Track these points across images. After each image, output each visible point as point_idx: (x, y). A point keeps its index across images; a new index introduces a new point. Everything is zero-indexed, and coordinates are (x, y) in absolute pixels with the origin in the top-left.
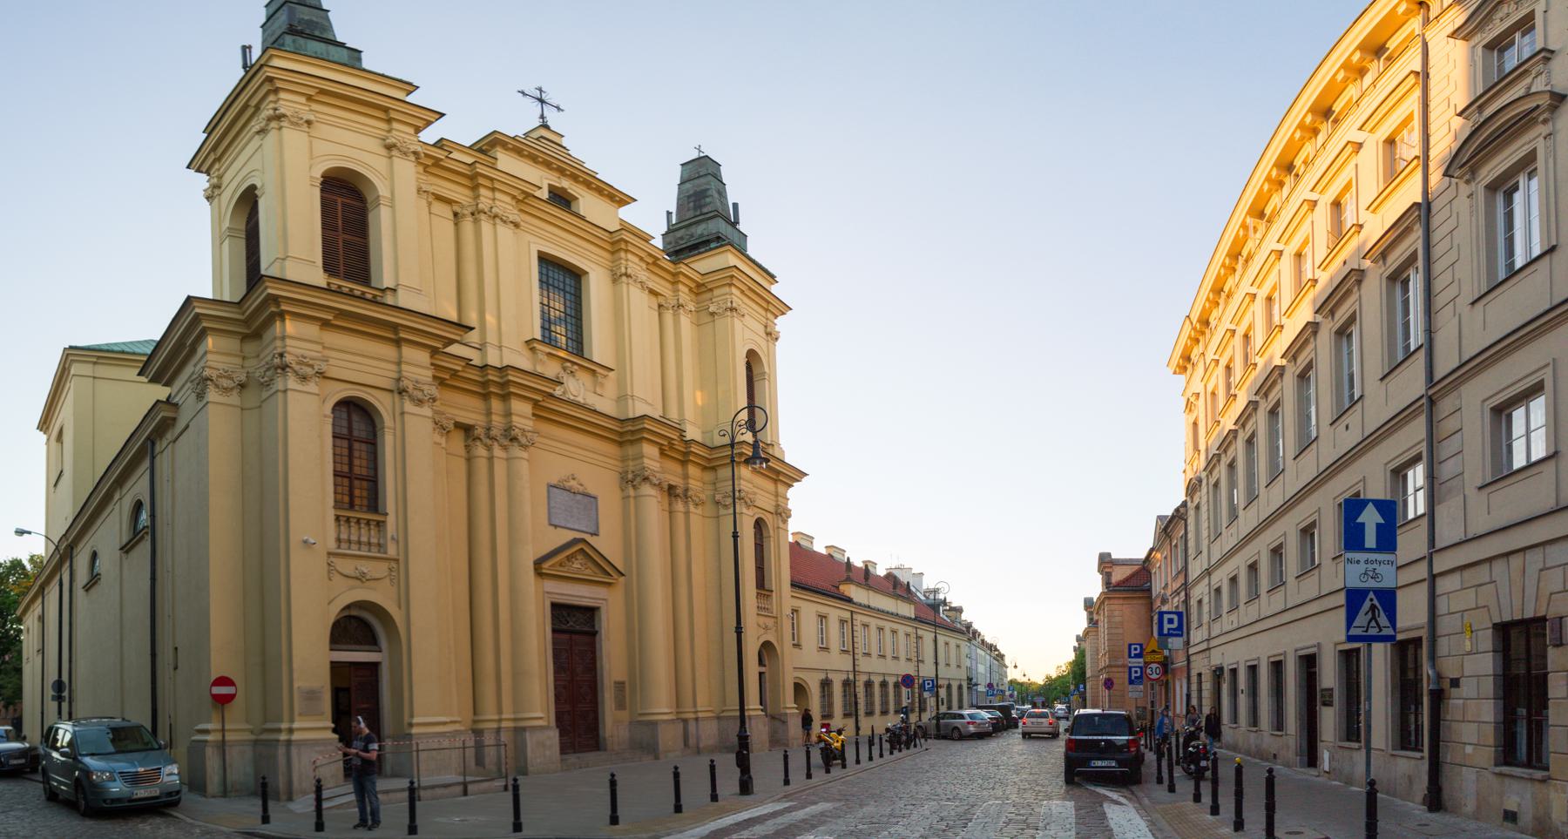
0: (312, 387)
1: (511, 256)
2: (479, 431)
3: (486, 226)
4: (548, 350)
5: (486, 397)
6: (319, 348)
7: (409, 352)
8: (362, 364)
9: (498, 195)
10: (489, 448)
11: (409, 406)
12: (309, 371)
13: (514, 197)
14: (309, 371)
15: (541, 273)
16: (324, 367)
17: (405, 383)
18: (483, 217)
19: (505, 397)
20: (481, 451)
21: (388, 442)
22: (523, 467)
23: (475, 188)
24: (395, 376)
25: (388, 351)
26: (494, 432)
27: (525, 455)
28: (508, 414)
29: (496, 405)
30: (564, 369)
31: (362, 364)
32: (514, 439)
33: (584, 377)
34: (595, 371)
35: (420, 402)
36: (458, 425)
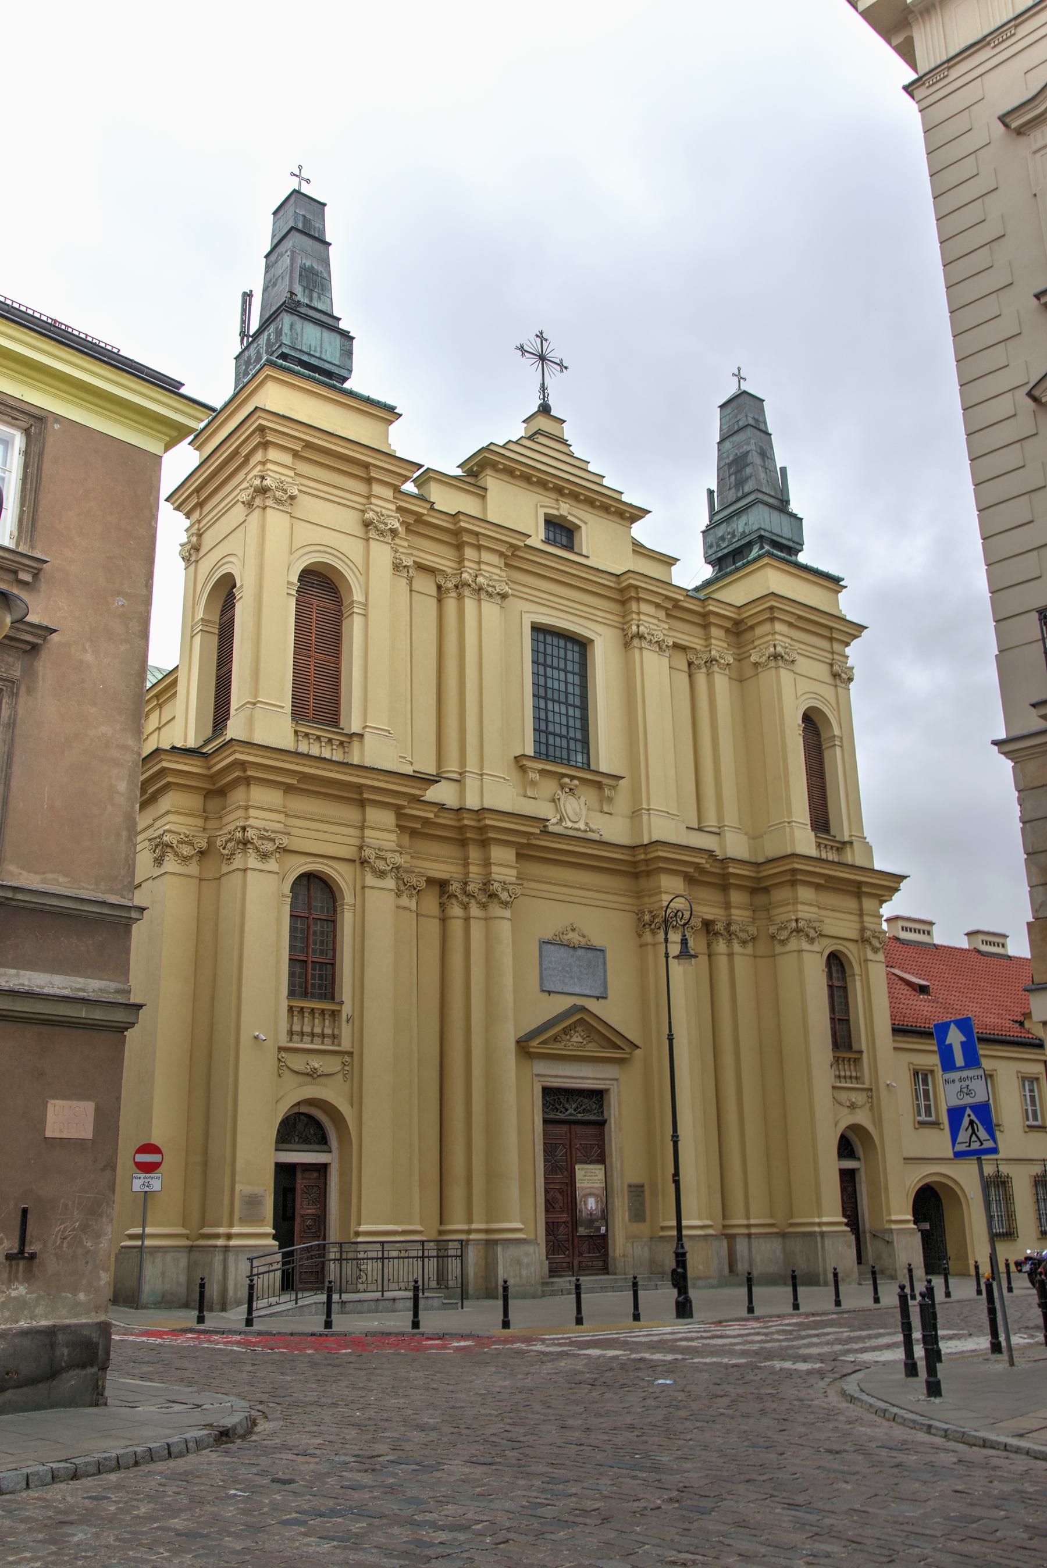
0: (272, 865)
1: (497, 640)
2: (455, 887)
3: (470, 604)
4: (540, 766)
5: (463, 843)
7: (374, 815)
8: (323, 836)
9: (486, 556)
10: (465, 907)
11: (370, 880)
12: (269, 846)
13: (501, 554)
14: (269, 846)
15: (535, 651)
16: (285, 841)
17: (367, 853)
18: (466, 592)
19: (484, 844)
20: (456, 911)
21: (347, 920)
22: (504, 929)
23: (459, 547)
24: (356, 842)
25: (351, 814)
26: (471, 888)
27: (507, 913)
28: (487, 863)
29: (474, 854)
30: (562, 787)
31: (323, 836)
32: (493, 896)
33: (588, 795)
34: (602, 784)
35: (381, 874)
36: (430, 881)
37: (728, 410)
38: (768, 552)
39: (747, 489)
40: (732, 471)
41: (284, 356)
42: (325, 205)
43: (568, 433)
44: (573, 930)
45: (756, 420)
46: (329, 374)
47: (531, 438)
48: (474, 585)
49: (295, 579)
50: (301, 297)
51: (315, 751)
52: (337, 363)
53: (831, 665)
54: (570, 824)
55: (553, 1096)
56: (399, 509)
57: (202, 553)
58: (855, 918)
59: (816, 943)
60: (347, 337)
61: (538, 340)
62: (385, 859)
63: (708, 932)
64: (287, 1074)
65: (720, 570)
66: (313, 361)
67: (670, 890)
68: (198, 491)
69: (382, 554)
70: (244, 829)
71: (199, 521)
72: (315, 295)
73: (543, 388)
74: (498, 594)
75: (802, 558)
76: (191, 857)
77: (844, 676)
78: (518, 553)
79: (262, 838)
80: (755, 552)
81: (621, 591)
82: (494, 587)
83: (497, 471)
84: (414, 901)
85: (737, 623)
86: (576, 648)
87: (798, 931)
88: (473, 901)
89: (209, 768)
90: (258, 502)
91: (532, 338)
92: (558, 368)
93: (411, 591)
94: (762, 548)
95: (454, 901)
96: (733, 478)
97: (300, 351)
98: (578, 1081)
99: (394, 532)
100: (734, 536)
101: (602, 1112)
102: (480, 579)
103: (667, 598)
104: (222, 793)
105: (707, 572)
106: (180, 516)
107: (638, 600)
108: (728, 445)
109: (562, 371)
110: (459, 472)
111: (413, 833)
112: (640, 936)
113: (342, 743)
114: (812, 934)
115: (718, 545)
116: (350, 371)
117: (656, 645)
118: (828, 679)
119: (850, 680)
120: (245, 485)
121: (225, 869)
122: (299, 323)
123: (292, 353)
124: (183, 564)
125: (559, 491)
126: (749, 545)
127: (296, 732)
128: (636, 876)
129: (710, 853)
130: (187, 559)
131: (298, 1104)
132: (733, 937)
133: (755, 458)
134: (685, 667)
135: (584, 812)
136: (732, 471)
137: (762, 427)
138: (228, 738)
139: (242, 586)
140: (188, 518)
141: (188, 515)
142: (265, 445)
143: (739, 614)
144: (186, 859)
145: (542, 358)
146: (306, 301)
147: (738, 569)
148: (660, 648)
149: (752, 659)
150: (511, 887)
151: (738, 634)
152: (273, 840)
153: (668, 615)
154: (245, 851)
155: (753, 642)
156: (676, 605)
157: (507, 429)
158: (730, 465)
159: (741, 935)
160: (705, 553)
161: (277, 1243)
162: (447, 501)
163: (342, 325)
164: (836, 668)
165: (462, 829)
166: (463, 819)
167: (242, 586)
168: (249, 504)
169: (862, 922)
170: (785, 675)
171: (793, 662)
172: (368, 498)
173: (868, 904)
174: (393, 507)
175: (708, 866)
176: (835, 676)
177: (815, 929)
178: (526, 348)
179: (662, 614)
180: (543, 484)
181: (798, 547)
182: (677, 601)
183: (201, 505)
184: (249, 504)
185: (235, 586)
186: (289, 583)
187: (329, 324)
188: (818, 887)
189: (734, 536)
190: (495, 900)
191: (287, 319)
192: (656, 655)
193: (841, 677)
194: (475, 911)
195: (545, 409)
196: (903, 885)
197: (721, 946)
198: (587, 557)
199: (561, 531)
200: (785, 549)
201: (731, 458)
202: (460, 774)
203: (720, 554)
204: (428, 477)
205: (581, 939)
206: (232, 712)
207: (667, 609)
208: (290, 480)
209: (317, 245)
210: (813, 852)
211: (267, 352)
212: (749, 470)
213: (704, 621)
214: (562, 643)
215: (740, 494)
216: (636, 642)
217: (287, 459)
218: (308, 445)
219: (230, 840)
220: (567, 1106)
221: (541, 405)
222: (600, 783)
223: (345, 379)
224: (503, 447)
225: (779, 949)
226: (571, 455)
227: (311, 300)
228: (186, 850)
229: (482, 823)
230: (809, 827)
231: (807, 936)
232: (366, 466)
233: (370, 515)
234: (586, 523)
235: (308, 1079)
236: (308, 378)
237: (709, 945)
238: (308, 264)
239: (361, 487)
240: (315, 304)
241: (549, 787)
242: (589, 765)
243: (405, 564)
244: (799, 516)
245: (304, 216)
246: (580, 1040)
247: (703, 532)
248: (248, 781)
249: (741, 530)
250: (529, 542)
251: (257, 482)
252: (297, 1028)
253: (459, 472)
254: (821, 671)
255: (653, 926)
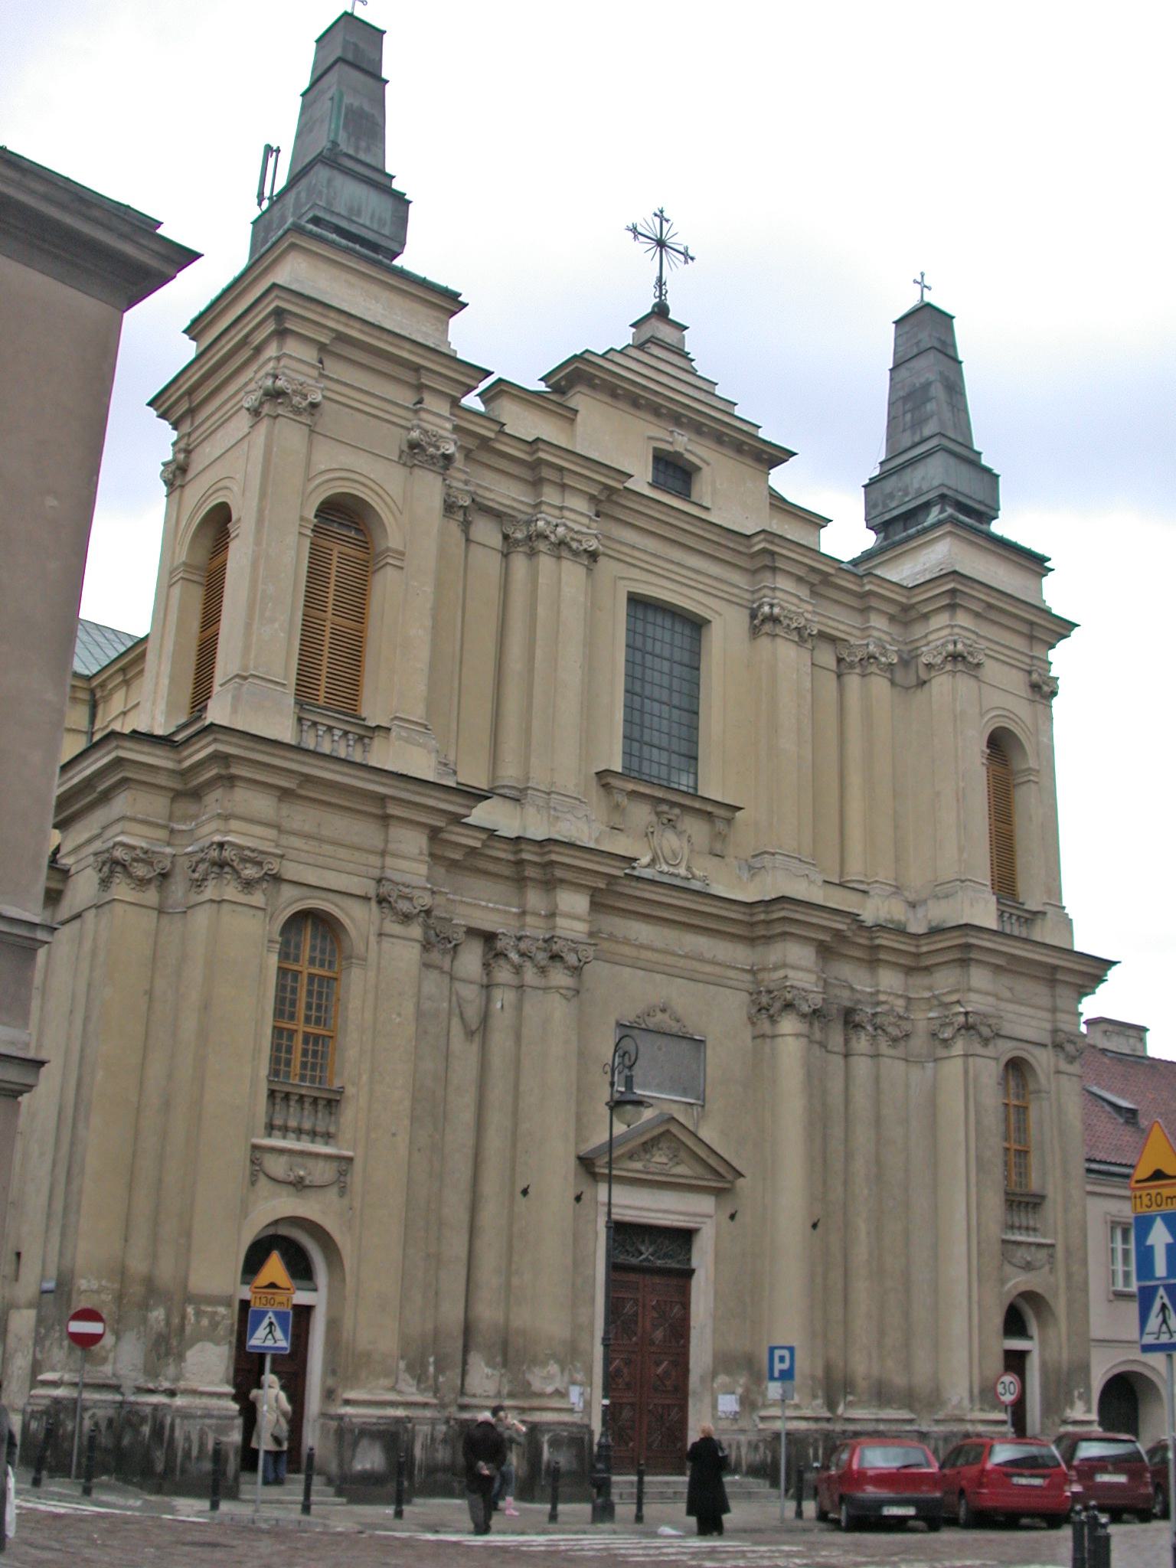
0: (258, 898)
3: (545, 562)
5: (520, 882)
6: (272, 833)
10: (518, 970)
13: (592, 498)
16: (275, 866)
18: (542, 546)
19: (550, 885)
29: (534, 899)
30: (658, 814)
31: (330, 860)
32: (555, 957)
35: (406, 918)
36: (472, 932)
37: (906, 328)
38: (951, 516)
39: (927, 432)
40: (908, 406)
41: (316, 221)
42: (384, 32)
43: (691, 343)
44: (663, 1010)
45: (943, 343)
46: (374, 247)
47: (640, 347)
48: (553, 538)
49: (310, 514)
50: (344, 147)
51: (326, 748)
52: (386, 231)
53: (1030, 673)
54: (665, 868)
55: (623, 1233)
56: (457, 429)
57: (191, 474)
58: (1047, 1015)
59: (991, 1047)
60: (401, 202)
61: (657, 220)
62: (411, 899)
63: (846, 1023)
64: (263, 1180)
65: (885, 538)
66: (353, 229)
67: (796, 964)
68: (190, 392)
69: (429, 489)
70: (221, 845)
71: (189, 434)
72: (363, 144)
73: (660, 283)
74: (585, 551)
75: (996, 528)
76: (150, 881)
77: (1046, 688)
78: (614, 498)
79: (244, 860)
80: (934, 515)
81: (753, 556)
82: (580, 542)
83: (594, 387)
84: (448, 959)
85: (906, 609)
86: (687, 632)
87: (968, 1027)
88: (528, 964)
89: (180, 762)
90: (266, 409)
91: (650, 217)
92: (682, 258)
93: (468, 540)
94: (942, 511)
95: (502, 962)
96: (908, 416)
97: (338, 214)
98: (660, 1215)
99: (448, 458)
100: (906, 494)
101: (689, 1260)
102: (561, 530)
103: (813, 569)
104: (196, 794)
105: (868, 540)
106: (165, 425)
107: (774, 569)
108: (903, 373)
109: (686, 262)
110: (542, 387)
111: (453, 865)
112: (753, 1024)
113: (361, 738)
114: (986, 1031)
115: (885, 505)
116: (403, 244)
117: (795, 633)
118: (1024, 691)
119: (1054, 693)
120: (253, 386)
121: (196, 898)
122: (340, 180)
123: (328, 217)
124: (164, 489)
125: (677, 419)
126: (926, 506)
127: (300, 720)
128: (752, 941)
129: (854, 917)
130: (170, 484)
131: (276, 1222)
132: (880, 1032)
133: (938, 391)
134: (833, 665)
135: (686, 851)
136: (908, 406)
137: (950, 352)
138: (207, 722)
139: (239, 520)
140: (175, 428)
141: (175, 426)
142: (281, 334)
143: (908, 598)
144: (142, 883)
145: (661, 244)
146: (351, 152)
147: (911, 538)
148: (800, 636)
149: (924, 660)
150: (581, 947)
151: (906, 624)
152: (260, 864)
153: (814, 593)
154: (219, 876)
155: (926, 636)
156: (824, 577)
157: (609, 332)
158: (905, 399)
159: (890, 1029)
160: (867, 514)
161: (237, 1407)
162: (524, 424)
163: (396, 185)
164: (1035, 676)
165: (520, 863)
166: (521, 851)
167: (239, 520)
168: (255, 412)
169: (1054, 1021)
170: (965, 684)
171: (978, 665)
172: (416, 412)
173: (1064, 993)
174: (449, 426)
175: (849, 934)
176: (1035, 687)
177: (989, 1026)
178: (640, 229)
179: (804, 592)
180: (656, 411)
181: (992, 513)
182: (827, 574)
183: (192, 412)
184: (255, 412)
185: (229, 519)
186: (302, 519)
187: (380, 182)
188: (997, 969)
189: (906, 494)
190: (558, 964)
191: (322, 173)
192: (793, 646)
193: (1043, 690)
194: (530, 975)
195: (661, 311)
196: (1112, 974)
197: (862, 1043)
198: (707, 509)
199: (674, 472)
200: (973, 512)
201: (907, 390)
202: (521, 791)
203: (887, 517)
204: (502, 389)
205: (673, 1024)
206: (216, 688)
207: (812, 585)
208: (311, 382)
209: (370, 81)
210: (992, 923)
211: (293, 215)
212: (930, 407)
213: (864, 603)
214: (668, 624)
215: (917, 439)
216: (767, 627)
217: (310, 354)
218: (341, 337)
219: (202, 860)
220: (643, 1249)
221: (655, 305)
222: (710, 813)
223: (396, 255)
224: (603, 356)
225: (941, 1052)
226: (693, 372)
227: (357, 149)
228: (140, 870)
229: (547, 858)
230: (989, 889)
231: (980, 1035)
232: (417, 369)
233: (415, 434)
234: (708, 464)
235: (291, 1189)
236: (347, 250)
237: (847, 1041)
238: (356, 104)
239: (407, 397)
240: (362, 156)
241: (641, 814)
242: (696, 789)
243: (461, 503)
244: (995, 471)
245: (355, 45)
246: (664, 1160)
247: (865, 486)
248: (231, 781)
249: (916, 486)
250: (629, 484)
251: (269, 382)
252: (278, 1122)
253: (542, 387)
254: (1016, 681)
255: (772, 1012)
